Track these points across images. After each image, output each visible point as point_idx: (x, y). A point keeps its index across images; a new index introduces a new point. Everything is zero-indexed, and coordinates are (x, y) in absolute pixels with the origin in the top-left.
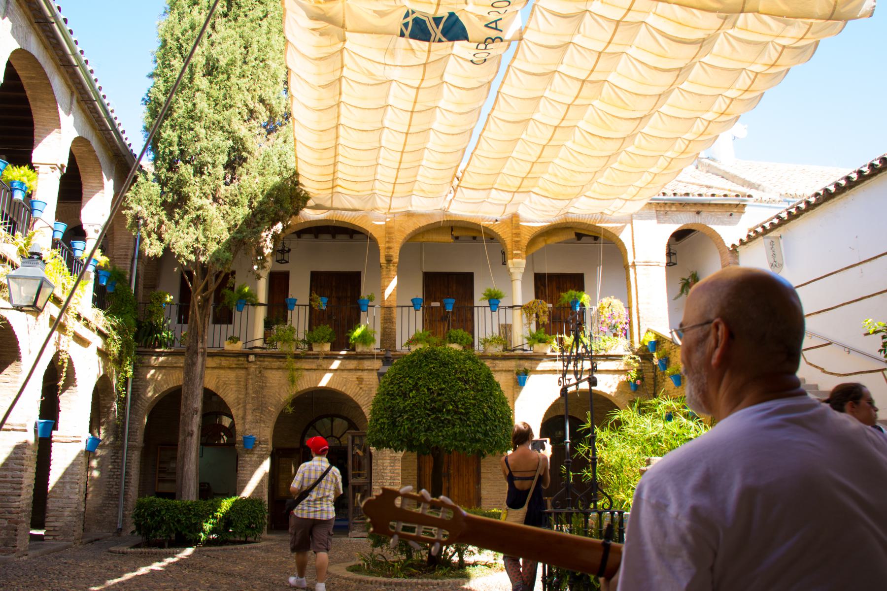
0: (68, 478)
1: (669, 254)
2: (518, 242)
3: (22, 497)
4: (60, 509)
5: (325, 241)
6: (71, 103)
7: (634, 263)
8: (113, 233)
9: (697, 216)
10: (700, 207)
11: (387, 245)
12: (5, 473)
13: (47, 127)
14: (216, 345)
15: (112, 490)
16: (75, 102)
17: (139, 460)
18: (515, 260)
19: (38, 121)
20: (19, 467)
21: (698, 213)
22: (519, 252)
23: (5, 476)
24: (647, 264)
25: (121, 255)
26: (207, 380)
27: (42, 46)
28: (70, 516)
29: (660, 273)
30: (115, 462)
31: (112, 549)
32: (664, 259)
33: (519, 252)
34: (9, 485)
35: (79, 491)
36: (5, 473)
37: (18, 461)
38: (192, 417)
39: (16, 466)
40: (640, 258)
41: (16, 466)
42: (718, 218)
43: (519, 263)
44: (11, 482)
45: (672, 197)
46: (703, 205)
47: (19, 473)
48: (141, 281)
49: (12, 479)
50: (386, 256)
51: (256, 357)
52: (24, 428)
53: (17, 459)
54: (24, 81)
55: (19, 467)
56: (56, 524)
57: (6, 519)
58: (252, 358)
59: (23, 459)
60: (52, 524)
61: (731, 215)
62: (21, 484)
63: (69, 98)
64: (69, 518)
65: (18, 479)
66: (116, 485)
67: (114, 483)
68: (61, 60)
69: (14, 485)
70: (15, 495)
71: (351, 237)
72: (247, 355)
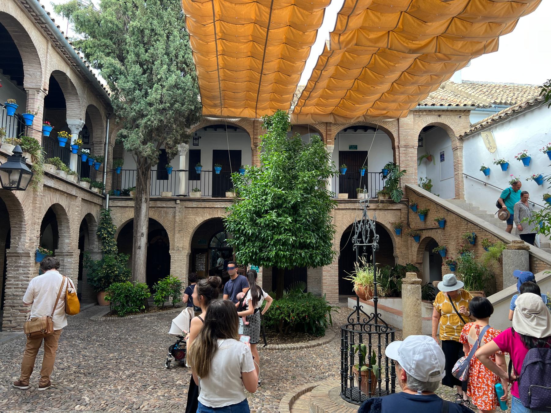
1: (420, 140)
2: (330, 135)
5: (220, 132)
6: (47, 48)
7: (398, 146)
8: (92, 128)
9: (438, 117)
10: (440, 112)
11: (255, 137)
12: (17, 282)
14: (157, 194)
16: (50, 47)
18: (328, 145)
20: (26, 279)
21: (439, 116)
22: (330, 141)
23: (18, 285)
24: (406, 146)
25: (98, 142)
26: (150, 215)
27: (19, 10)
29: (414, 153)
31: (91, 318)
32: (416, 143)
33: (330, 141)
34: (20, 289)
36: (17, 282)
37: (25, 275)
38: (140, 239)
40: (402, 143)
41: (24, 278)
42: (452, 119)
43: (330, 147)
44: (21, 288)
45: (424, 107)
46: (443, 111)
47: (26, 282)
48: (111, 157)
50: (254, 143)
51: (180, 200)
52: (28, 255)
54: (12, 34)
55: (26, 279)
58: (178, 202)
59: (28, 274)
61: (460, 117)
63: (46, 45)
68: (36, 19)
71: (236, 130)
72: (175, 200)
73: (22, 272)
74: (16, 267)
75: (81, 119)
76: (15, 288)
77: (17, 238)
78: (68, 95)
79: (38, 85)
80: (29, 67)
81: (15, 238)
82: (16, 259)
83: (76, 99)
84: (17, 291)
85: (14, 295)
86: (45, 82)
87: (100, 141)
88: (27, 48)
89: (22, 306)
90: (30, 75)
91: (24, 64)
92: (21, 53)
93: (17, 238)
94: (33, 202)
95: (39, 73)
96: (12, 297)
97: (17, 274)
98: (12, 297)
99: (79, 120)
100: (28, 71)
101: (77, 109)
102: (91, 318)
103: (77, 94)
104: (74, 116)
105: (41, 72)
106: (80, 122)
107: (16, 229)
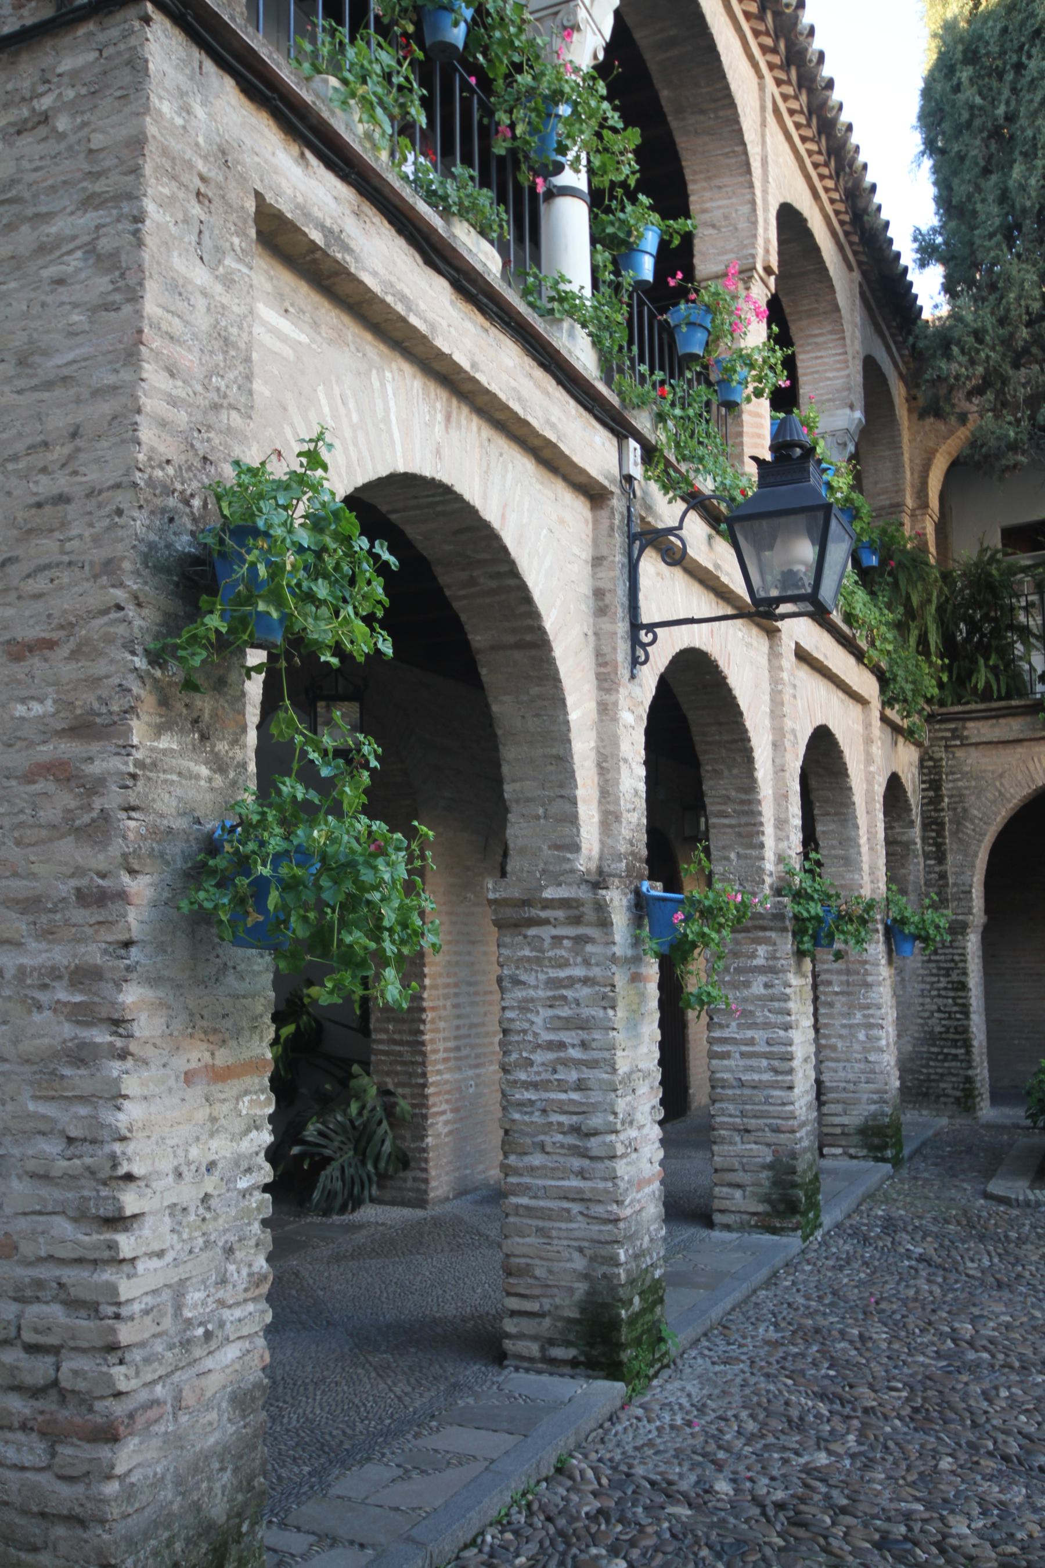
0: (859, 1015)
3: (796, 1090)
4: (851, 1087)
12: (749, 1034)
13: (717, 182)
15: (930, 1022)
17: (980, 953)
19: (695, 173)
23: (751, 1042)
28: (875, 1102)
30: (929, 961)
31: (996, 1187)
34: (764, 1063)
35: (888, 1045)
36: (749, 1034)
37: (776, 1004)
39: (772, 1017)
41: (772, 1017)
44: (767, 1056)
47: (782, 1033)
49: (768, 1049)
53: (772, 999)
56: (844, 1120)
57: (768, 1145)
60: (837, 1120)
62: (791, 1059)
64: (873, 1107)
65: (783, 1049)
66: (939, 1011)
67: (935, 1007)
69: (776, 1063)
70: (781, 1088)
73: (762, 991)
74: (739, 971)
75: (852, 407)
76: (743, 1055)
77: (733, 856)
78: (804, 323)
79: (746, 257)
80: (708, 194)
81: (727, 859)
82: (736, 942)
83: (831, 332)
84: (751, 1069)
85: (742, 1084)
86: (767, 241)
87: (892, 506)
88: (702, 112)
89: (777, 1130)
90: (713, 226)
91: (691, 187)
92: (682, 142)
93: (733, 856)
94: (772, 711)
95: (746, 209)
96: (738, 1092)
97: (745, 1000)
98: (738, 1092)
99: (848, 411)
100: (704, 211)
101: (838, 370)
102: (996, 1187)
103: (837, 309)
104: (829, 400)
105: (753, 203)
106: (851, 420)
107: (726, 821)
